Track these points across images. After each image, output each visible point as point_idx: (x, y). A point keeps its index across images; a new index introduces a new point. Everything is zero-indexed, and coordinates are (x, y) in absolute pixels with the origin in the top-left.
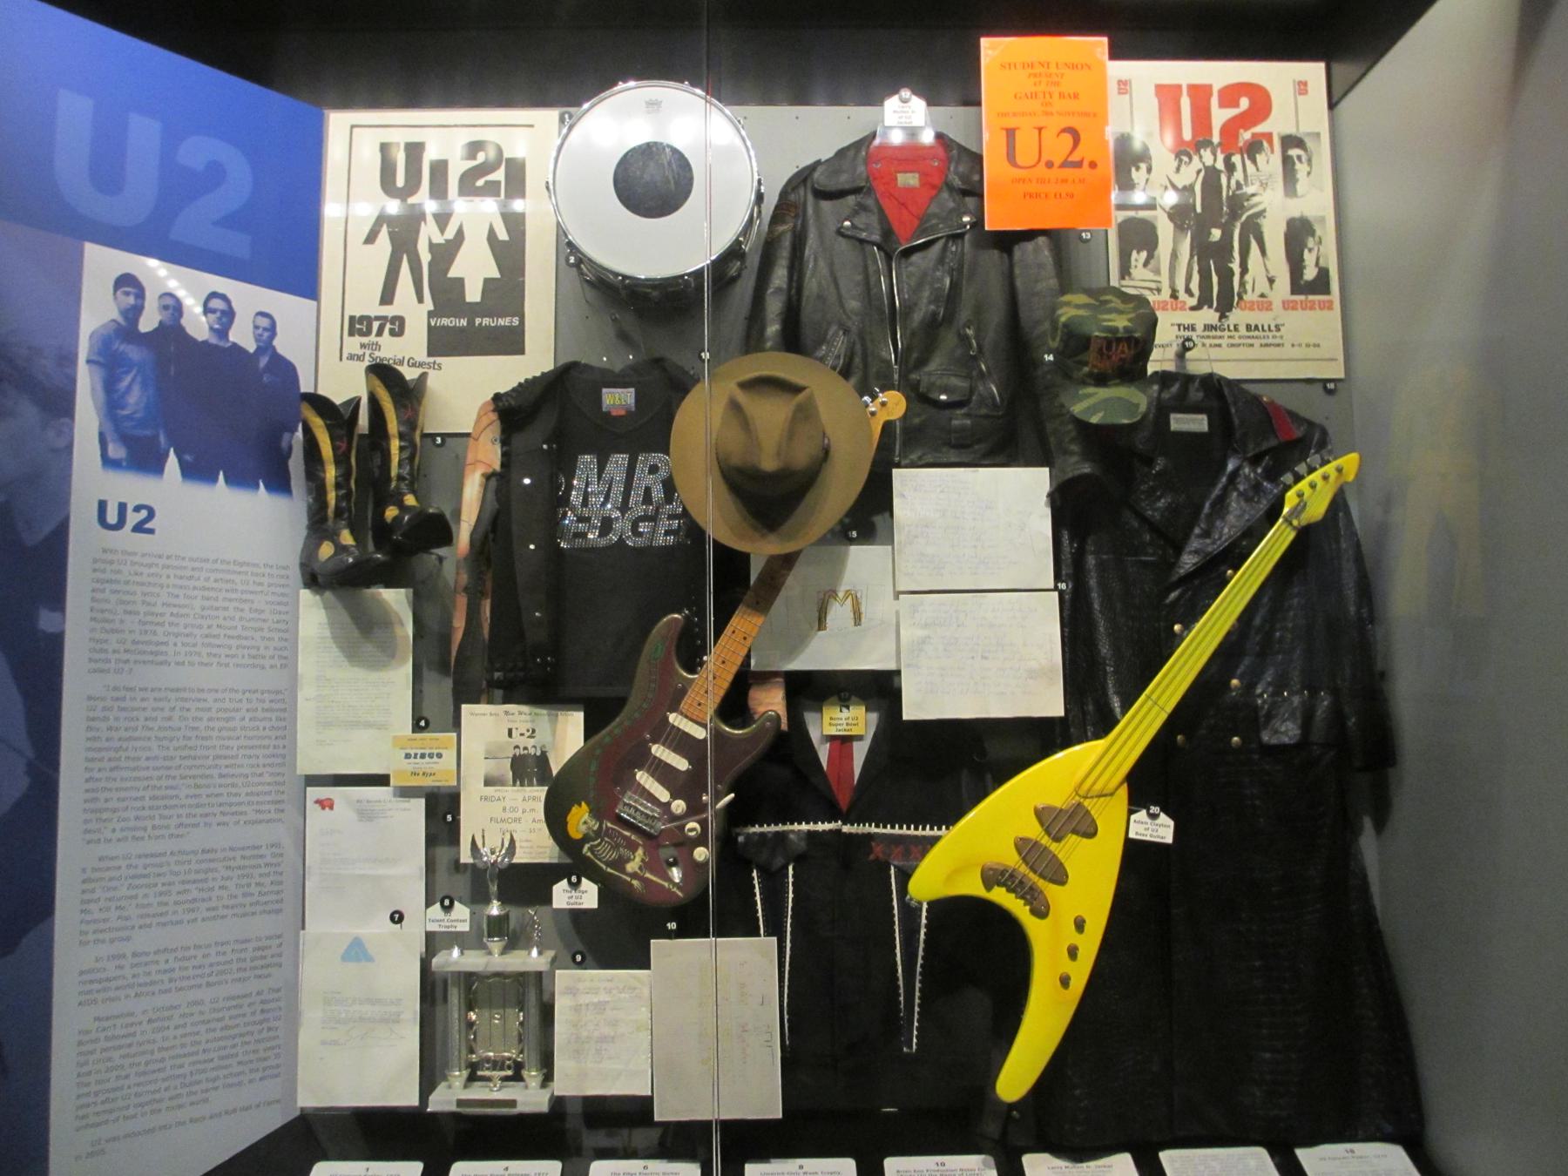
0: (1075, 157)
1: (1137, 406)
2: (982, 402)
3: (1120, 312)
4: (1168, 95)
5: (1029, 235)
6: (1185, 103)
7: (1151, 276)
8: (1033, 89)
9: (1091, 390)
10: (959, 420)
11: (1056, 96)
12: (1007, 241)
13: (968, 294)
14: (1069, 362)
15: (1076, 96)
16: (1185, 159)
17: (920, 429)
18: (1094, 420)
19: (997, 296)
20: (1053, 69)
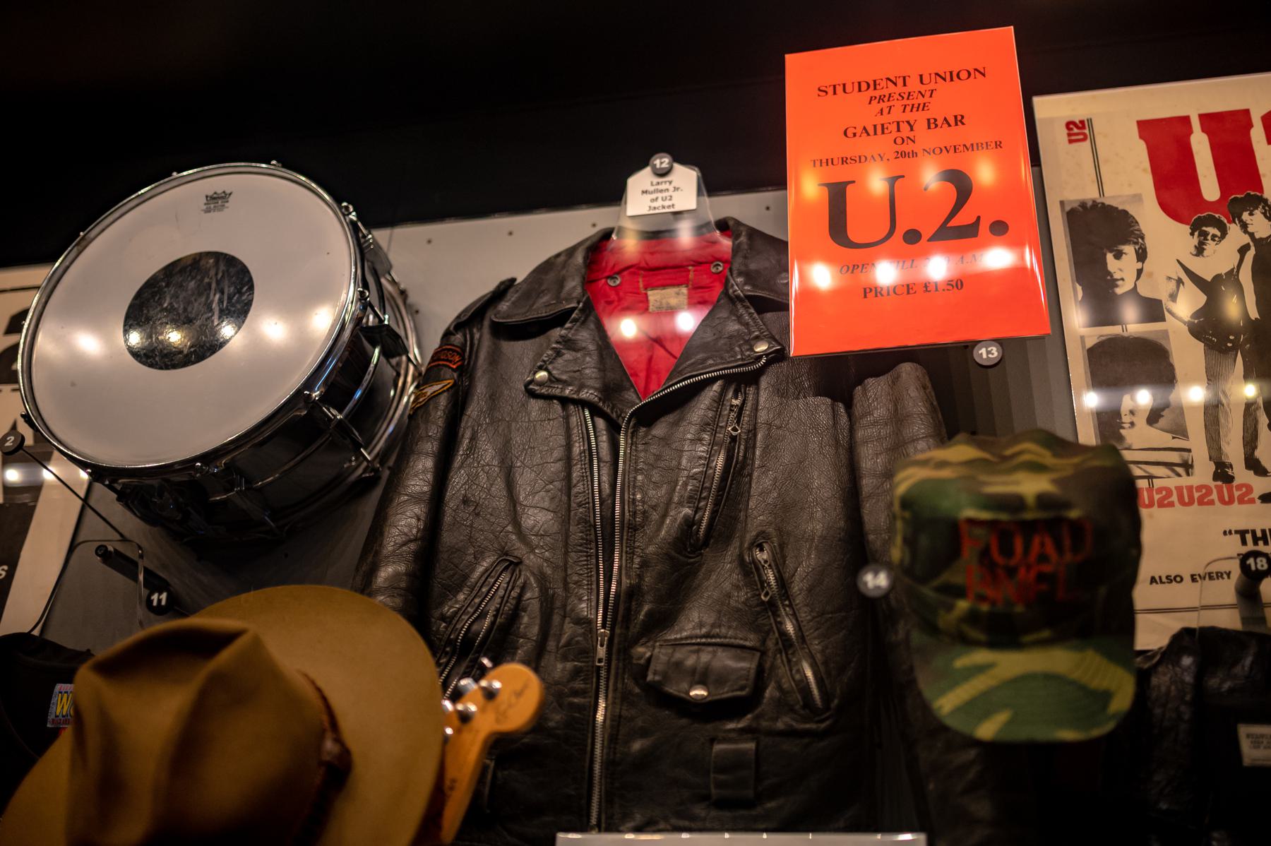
0: (963, 218)
1: (1105, 697)
2: (782, 705)
3: (1036, 468)
4: (1166, 140)
5: (880, 362)
6: (1200, 145)
7: (1167, 440)
8: (879, 120)
9: (981, 656)
10: (731, 742)
11: (921, 125)
12: (840, 376)
13: (763, 486)
14: (927, 591)
15: (959, 120)
16: (1212, 231)
17: (644, 762)
18: (987, 730)
19: (822, 483)
20: (913, 85)
